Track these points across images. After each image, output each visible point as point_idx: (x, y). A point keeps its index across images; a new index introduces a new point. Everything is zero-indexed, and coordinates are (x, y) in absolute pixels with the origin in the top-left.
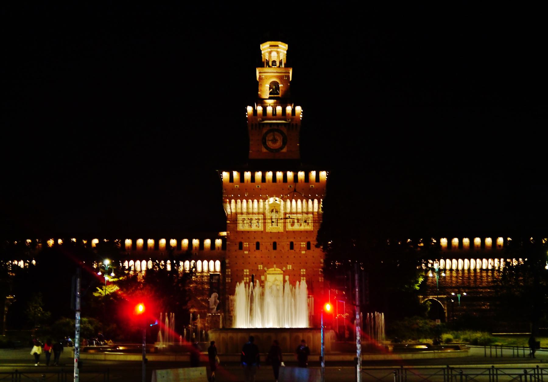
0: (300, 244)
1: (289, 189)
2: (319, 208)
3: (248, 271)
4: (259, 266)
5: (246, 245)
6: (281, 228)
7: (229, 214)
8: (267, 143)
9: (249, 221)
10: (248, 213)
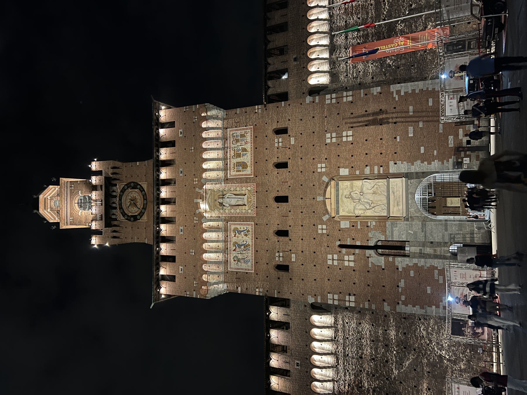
0: (278, 148)
1: (186, 175)
2: (216, 118)
3: (330, 257)
4: (320, 232)
5: (279, 256)
6: (249, 188)
7: (227, 287)
8: (136, 214)
9: (238, 249)
10: (225, 251)
